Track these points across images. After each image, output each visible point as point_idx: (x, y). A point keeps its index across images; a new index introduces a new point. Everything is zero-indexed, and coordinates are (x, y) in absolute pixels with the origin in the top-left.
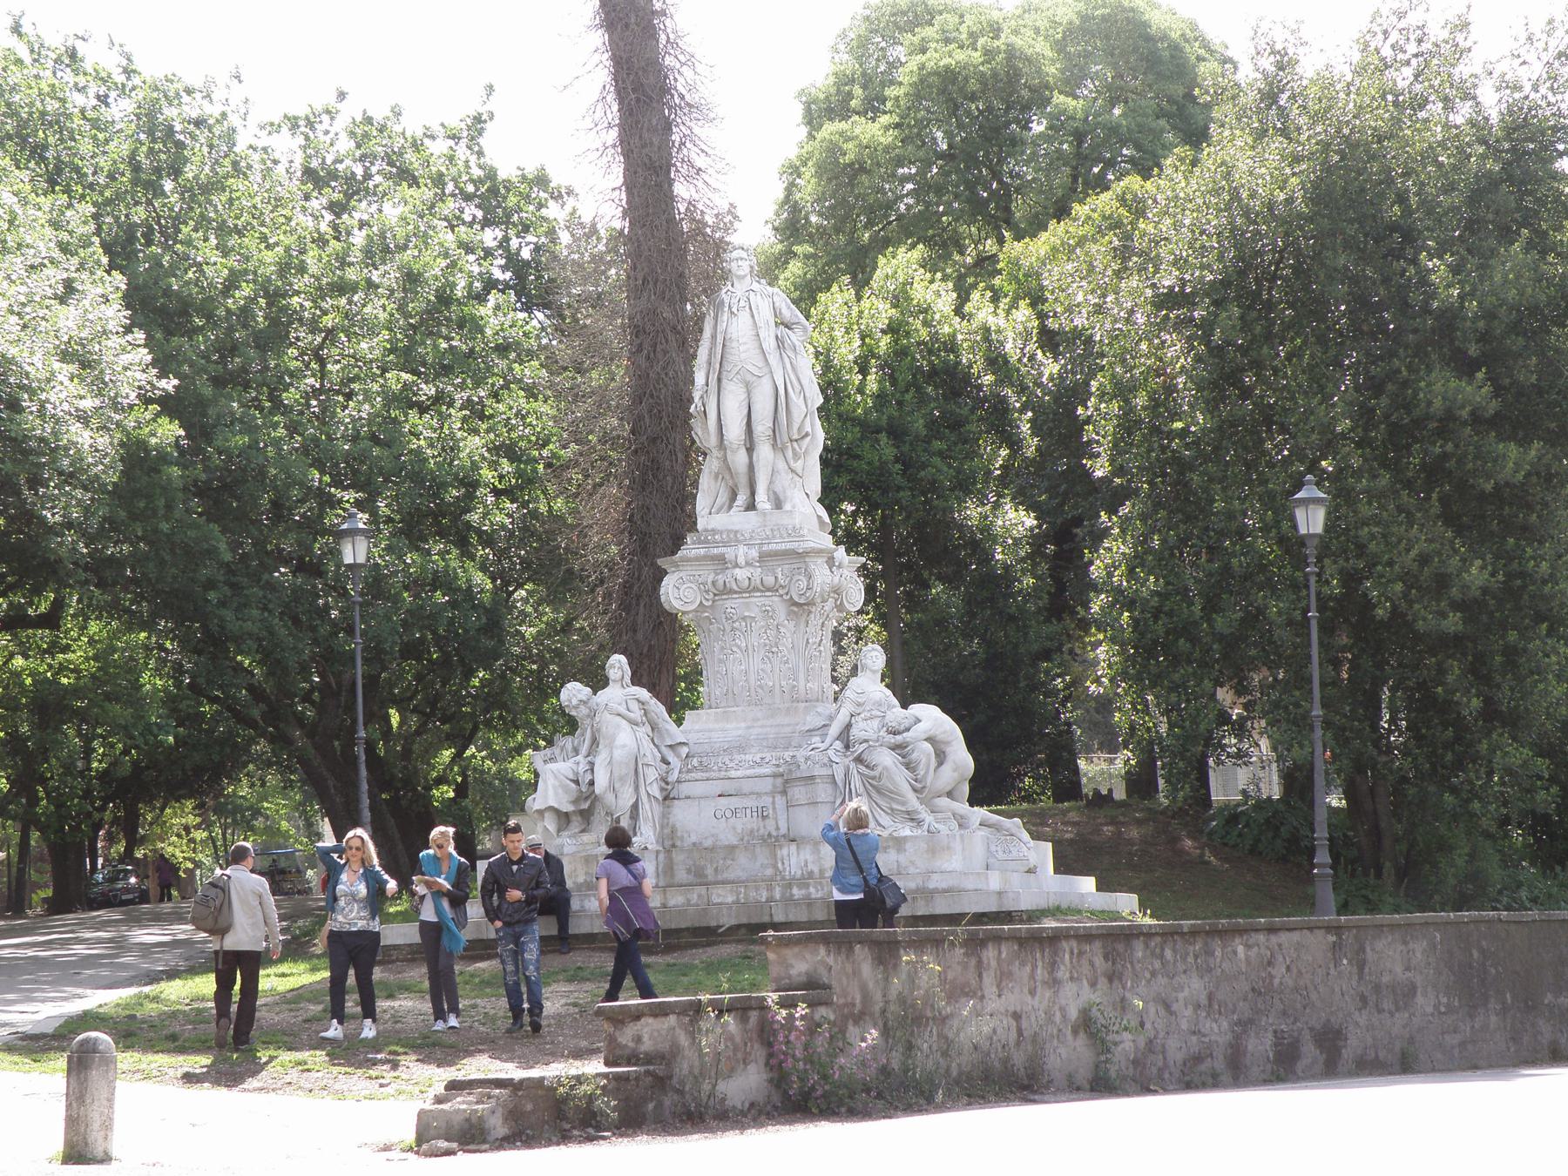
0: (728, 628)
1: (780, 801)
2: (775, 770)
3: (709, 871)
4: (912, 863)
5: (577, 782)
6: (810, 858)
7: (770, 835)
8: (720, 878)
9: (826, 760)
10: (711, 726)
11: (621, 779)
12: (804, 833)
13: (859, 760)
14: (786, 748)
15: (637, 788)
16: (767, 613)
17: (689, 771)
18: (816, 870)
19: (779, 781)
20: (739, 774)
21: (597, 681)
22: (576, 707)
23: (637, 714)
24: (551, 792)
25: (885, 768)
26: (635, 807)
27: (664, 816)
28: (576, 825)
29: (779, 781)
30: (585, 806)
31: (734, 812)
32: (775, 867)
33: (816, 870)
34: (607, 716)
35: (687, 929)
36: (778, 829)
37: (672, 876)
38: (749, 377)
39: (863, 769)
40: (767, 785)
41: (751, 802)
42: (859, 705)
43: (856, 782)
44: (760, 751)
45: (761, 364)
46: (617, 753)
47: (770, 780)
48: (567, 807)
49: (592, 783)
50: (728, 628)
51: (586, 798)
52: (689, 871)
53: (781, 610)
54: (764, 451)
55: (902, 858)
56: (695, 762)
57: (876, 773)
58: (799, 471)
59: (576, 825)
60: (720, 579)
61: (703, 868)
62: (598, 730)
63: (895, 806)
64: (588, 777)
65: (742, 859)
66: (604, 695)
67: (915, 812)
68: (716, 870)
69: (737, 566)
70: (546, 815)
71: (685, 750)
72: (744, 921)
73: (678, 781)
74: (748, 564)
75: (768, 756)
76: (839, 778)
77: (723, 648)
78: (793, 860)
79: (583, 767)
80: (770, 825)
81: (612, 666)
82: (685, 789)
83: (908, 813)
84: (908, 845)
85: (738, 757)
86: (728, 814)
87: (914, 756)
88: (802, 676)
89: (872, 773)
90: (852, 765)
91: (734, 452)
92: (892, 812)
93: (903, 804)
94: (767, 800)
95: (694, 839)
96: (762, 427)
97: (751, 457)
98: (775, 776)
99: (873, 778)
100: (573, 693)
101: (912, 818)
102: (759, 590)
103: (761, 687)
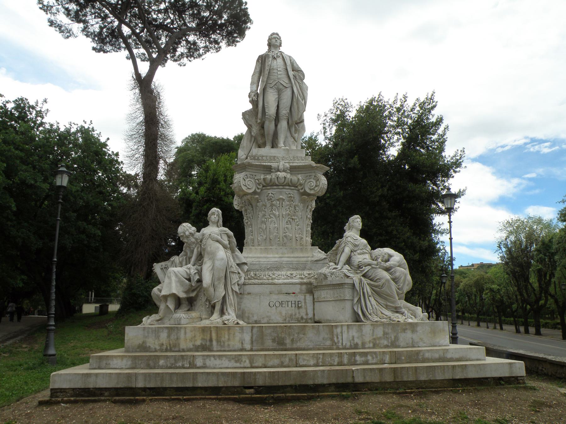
0: (268, 205)
1: (309, 298)
2: (301, 280)
3: (288, 341)
4: (421, 339)
5: (189, 280)
6: (356, 335)
7: (302, 318)
8: (295, 346)
9: (342, 275)
10: (259, 255)
11: (219, 279)
12: (329, 318)
13: (364, 276)
14: (304, 269)
15: (226, 286)
16: (291, 199)
17: (249, 279)
18: (360, 343)
19: (304, 287)
20: (280, 281)
21: (201, 222)
22: (187, 237)
23: (226, 242)
24: (174, 284)
25: (387, 280)
26: (224, 297)
27: (239, 304)
28: (185, 306)
29: (304, 287)
30: (193, 295)
31: (281, 304)
32: (332, 339)
33: (360, 343)
34: (210, 242)
35: (291, 386)
36: (307, 314)
37: (263, 343)
38: (281, 87)
39: (369, 281)
40: (297, 289)
41: (291, 298)
42: (356, 246)
43: (368, 289)
44: (288, 270)
45: (287, 81)
46: (217, 263)
47: (299, 286)
48: (182, 295)
49: (200, 281)
50: (268, 205)
51: (193, 291)
52: (274, 340)
53: (297, 197)
54: (283, 124)
55: (415, 336)
56: (252, 274)
57: (380, 283)
58: (296, 139)
59: (185, 306)
60: (268, 177)
61: (283, 339)
62: (204, 250)
63: (389, 304)
64: (197, 277)
65: (311, 334)
66: (205, 231)
67: (400, 307)
68: (292, 340)
69: (278, 170)
70: (169, 299)
71: (246, 268)
72: (334, 381)
73: (244, 284)
74: (284, 171)
75: (294, 273)
76: (357, 286)
77: (264, 215)
78: (345, 336)
79: (193, 271)
80: (303, 312)
81: (213, 214)
82: (248, 289)
83: (396, 308)
84: (419, 328)
85: (277, 273)
86: (277, 304)
87: (398, 274)
88: (305, 233)
89: (376, 284)
90: (363, 278)
91: (270, 121)
92: (387, 307)
93: (393, 302)
94: (301, 298)
95: (255, 318)
96: (284, 112)
97: (276, 126)
98: (301, 284)
99: (376, 287)
100: (186, 228)
101: (397, 310)
102: (289, 186)
103: (286, 236)
